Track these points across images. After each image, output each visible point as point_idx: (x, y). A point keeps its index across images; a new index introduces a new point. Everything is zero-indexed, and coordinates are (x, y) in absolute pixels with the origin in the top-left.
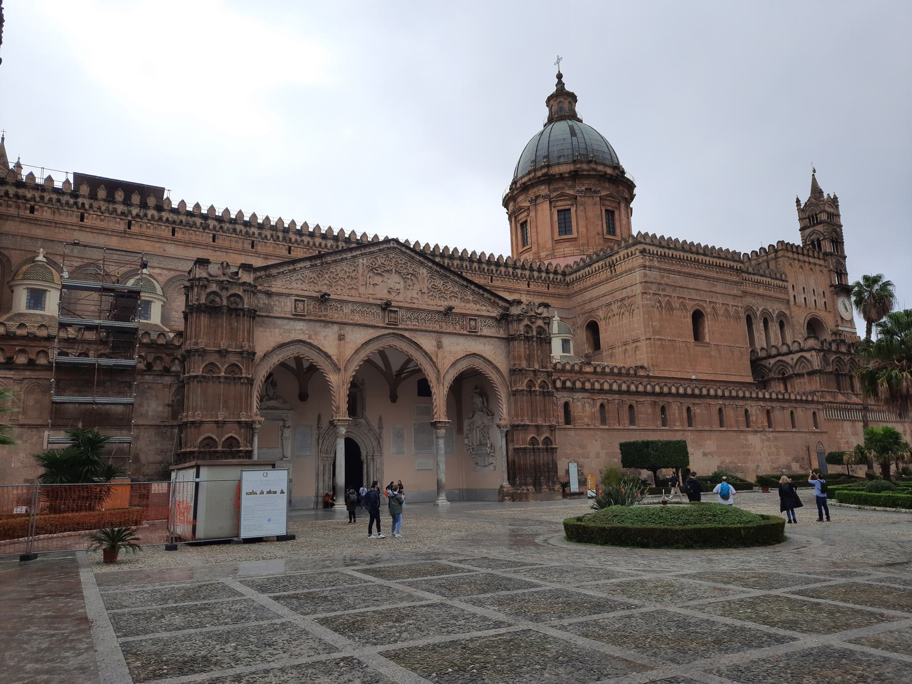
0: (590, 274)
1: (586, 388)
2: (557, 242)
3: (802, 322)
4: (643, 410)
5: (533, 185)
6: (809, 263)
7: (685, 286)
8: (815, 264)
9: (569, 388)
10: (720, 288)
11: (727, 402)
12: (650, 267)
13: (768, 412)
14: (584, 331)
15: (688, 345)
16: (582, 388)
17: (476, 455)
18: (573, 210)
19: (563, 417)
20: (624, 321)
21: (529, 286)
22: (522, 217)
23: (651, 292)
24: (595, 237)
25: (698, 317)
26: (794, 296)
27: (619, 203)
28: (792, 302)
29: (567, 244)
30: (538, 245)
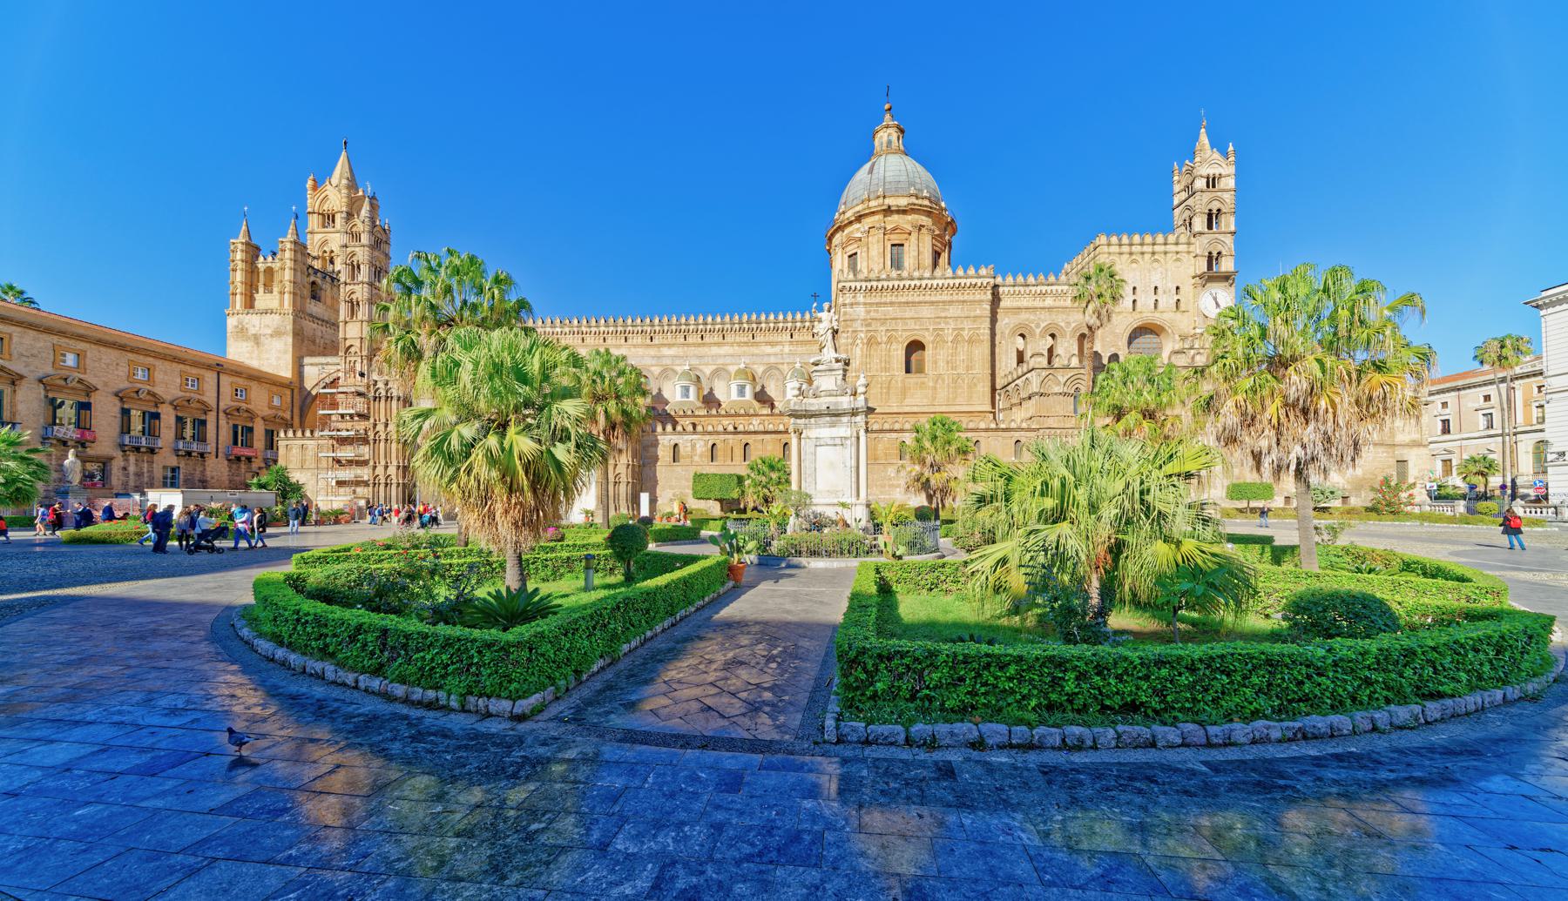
10: (953, 311)
12: (852, 304)
21: (792, 337)
27: (910, 234)
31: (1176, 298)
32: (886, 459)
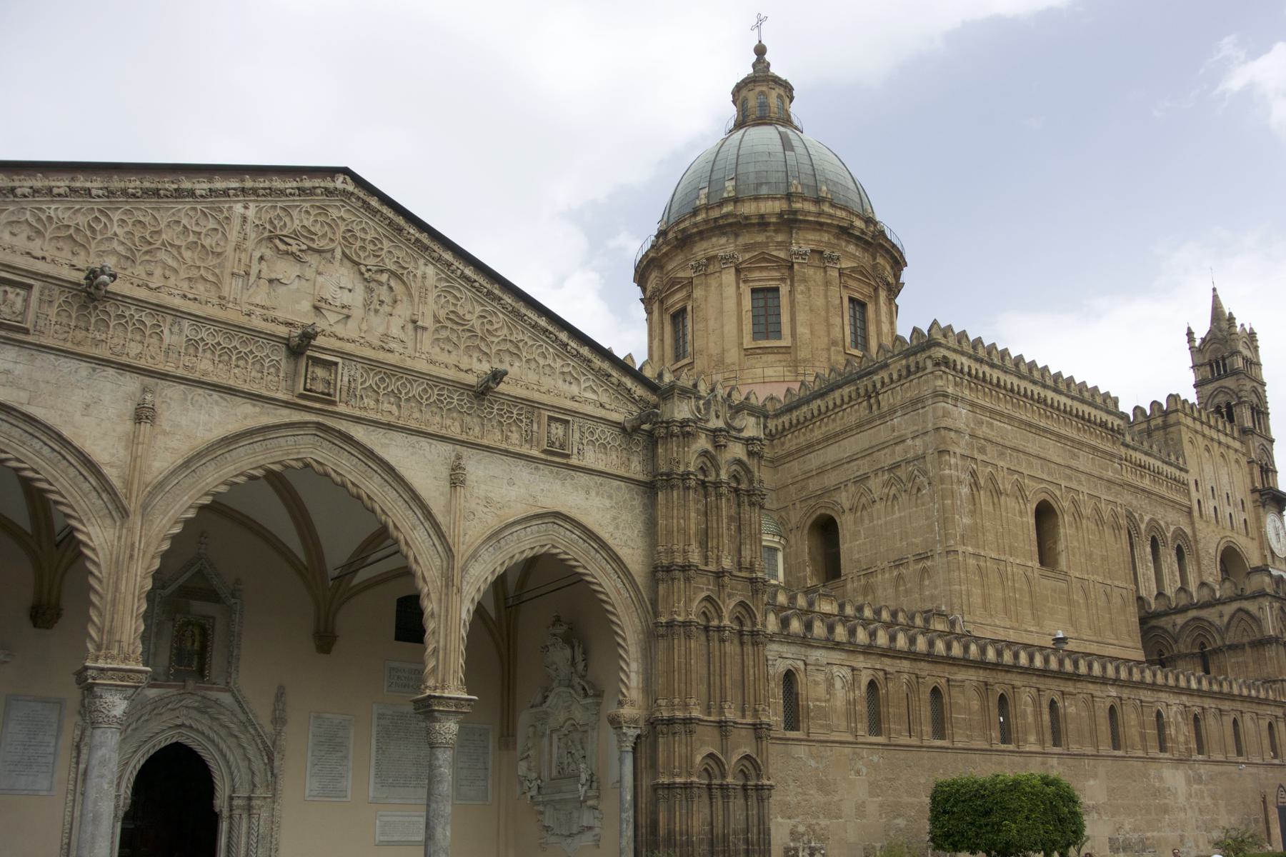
0: (821, 415)
1: (838, 639)
2: (749, 352)
3: (1212, 551)
4: (961, 701)
5: (703, 234)
6: (1220, 443)
7: (1021, 448)
8: (1228, 447)
9: (797, 636)
10: (1084, 462)
11: (1125, 693)
13: (1196, 719)
14: (806, 537)
15: (1029, 573)
16: (827, 639)
17: (545, 804)
18: (784, 290)
19: (781, 709)
20: (897, 515)
22: (676, 300)
23: (958, 451)
24: (829, 350)
25: (1045, 513)
26: (1199, 501)
27: (876, 290)
28: (1196, 514)
29: (771, 358)
30: (710, 356)
31: (1243, 516)
32: (1145, 749)
